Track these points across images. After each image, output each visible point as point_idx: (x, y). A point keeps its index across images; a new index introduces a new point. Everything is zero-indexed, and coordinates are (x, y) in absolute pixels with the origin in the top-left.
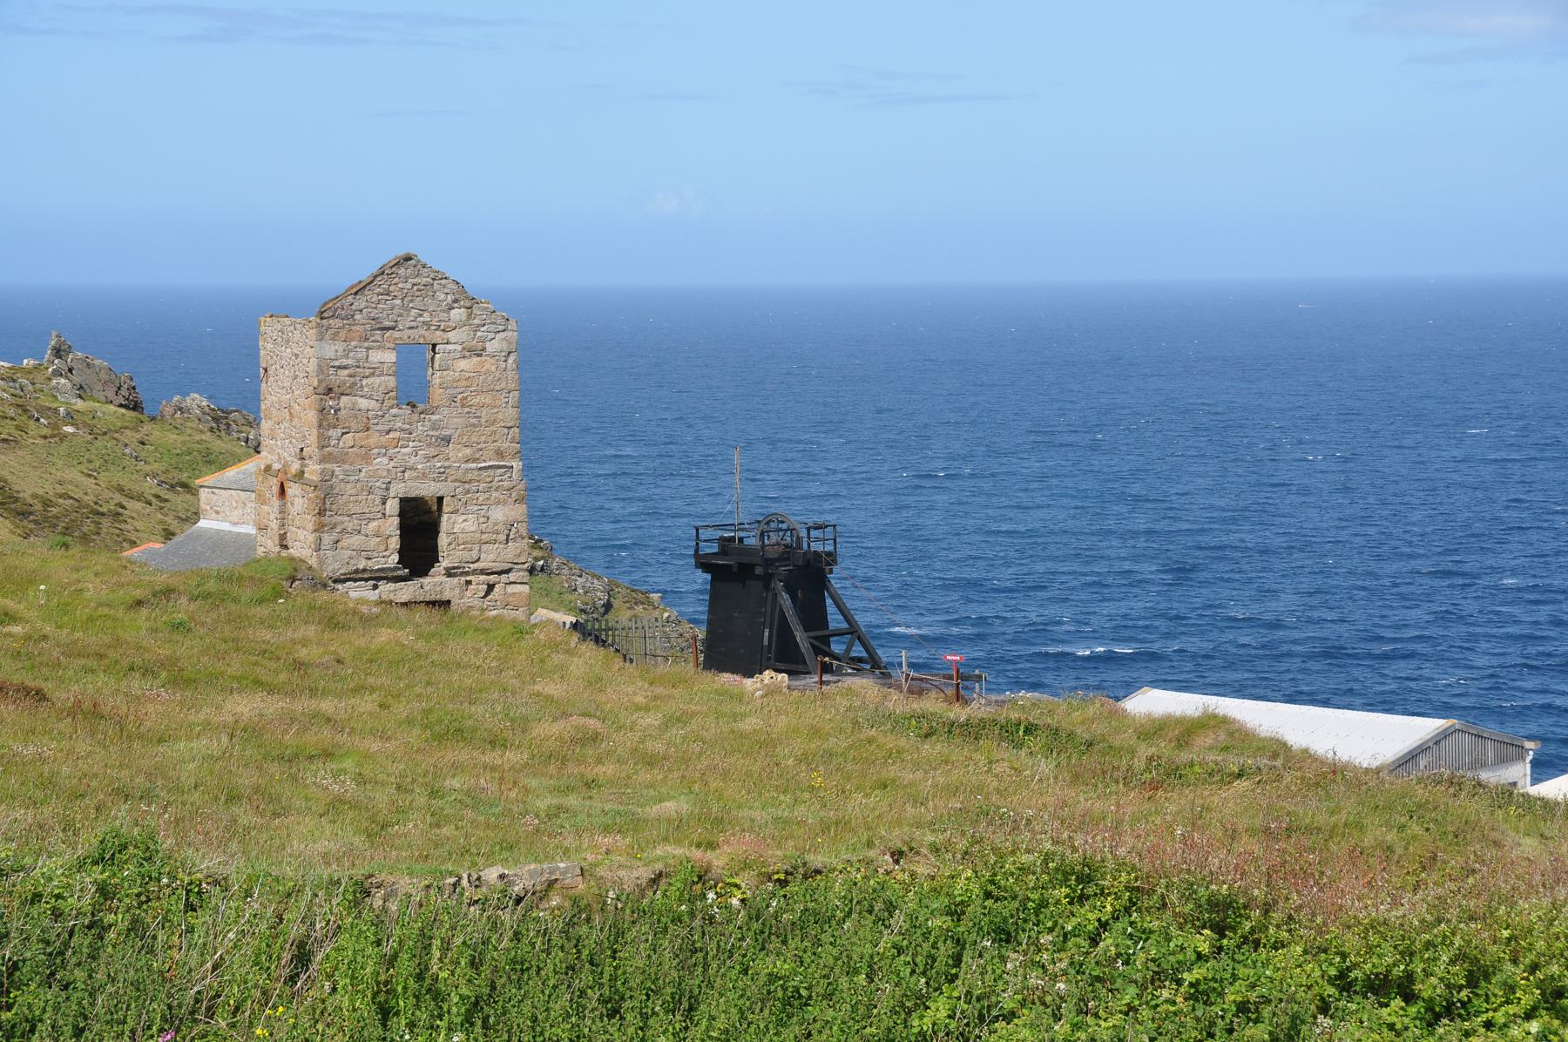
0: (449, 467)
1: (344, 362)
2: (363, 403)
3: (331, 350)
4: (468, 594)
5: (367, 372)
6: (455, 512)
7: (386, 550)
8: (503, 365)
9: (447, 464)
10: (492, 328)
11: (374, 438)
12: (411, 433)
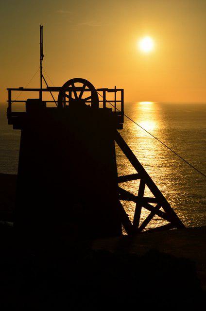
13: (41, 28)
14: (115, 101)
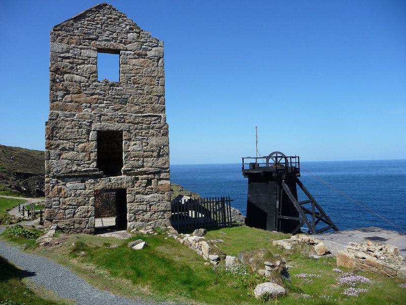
0: (126, 115)
1: (67, 55)
2: (77, 78)
3: (60, 47)
4: (137, 185)
5: (80, 61)
6: (130, 140)
9: (125, 113)
10: (151, 44)
11: (83, 98)
13: (256, 127)
14: (296, 163)
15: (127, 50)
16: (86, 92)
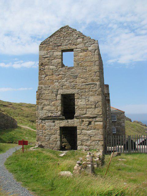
0: (76, 85)
1: (47, 56)
2: (51, 67)
3: (43, 52)
4: (83, 124)
5: (53, 58)
6: (78, 98)
7: (57, 110)
8: (93, 53)
10: (90, 43)
11: (55, 77)
12: (65, 75)
15: (77, 48)
16: (56, 74)
